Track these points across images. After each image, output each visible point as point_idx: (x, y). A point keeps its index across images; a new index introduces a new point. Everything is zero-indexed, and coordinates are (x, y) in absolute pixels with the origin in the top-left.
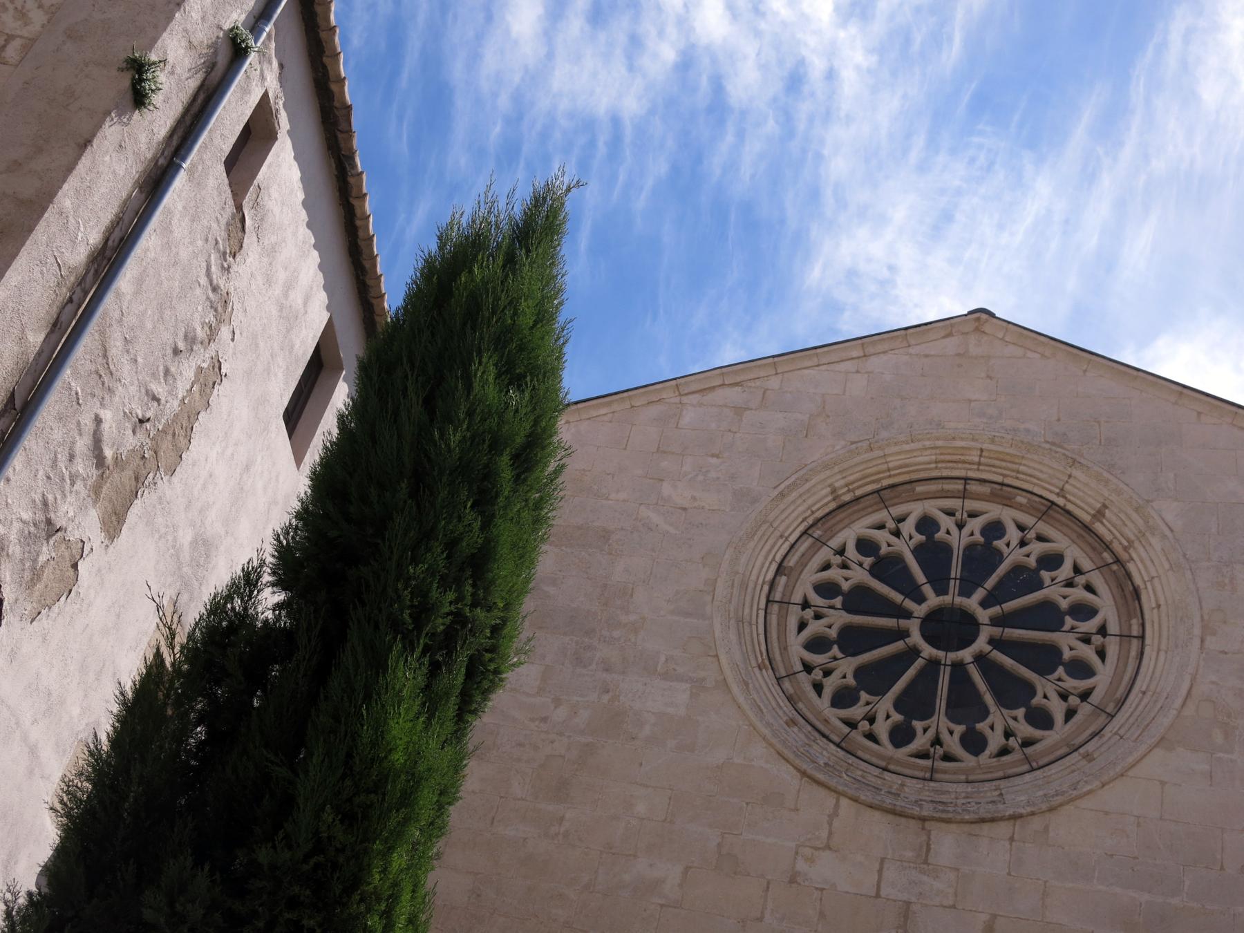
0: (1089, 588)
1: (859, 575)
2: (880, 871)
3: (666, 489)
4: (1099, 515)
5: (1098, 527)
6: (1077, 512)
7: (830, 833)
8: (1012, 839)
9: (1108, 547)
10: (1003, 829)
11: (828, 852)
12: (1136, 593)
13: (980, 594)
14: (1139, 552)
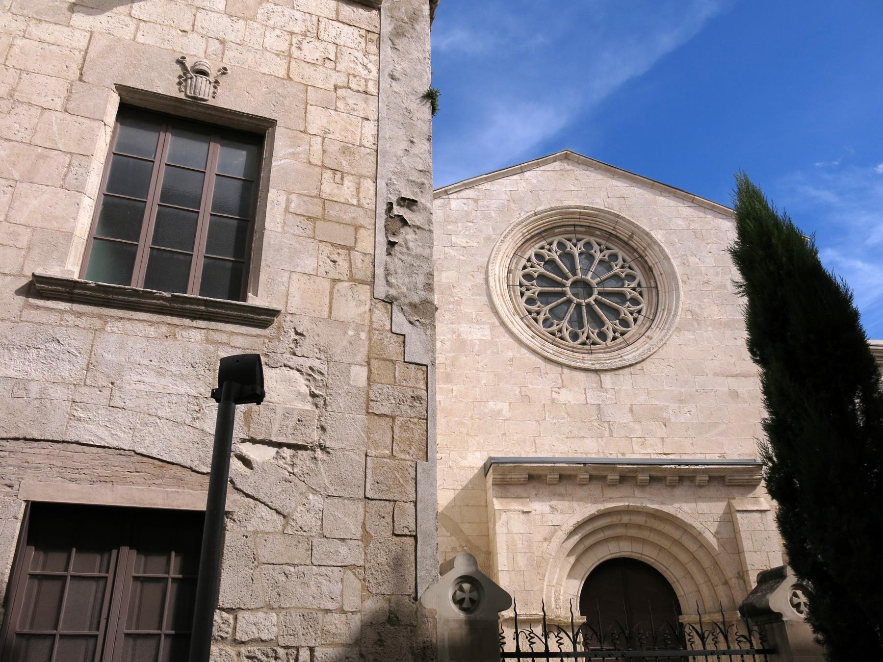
1: (541, 269)
4: (631, 237)
5: (631, 242)
6: (621, 237)
9: (636, 250)
10: (627, 370)
12: (651, 269)
13: (590, 274)
14: (649, 252)
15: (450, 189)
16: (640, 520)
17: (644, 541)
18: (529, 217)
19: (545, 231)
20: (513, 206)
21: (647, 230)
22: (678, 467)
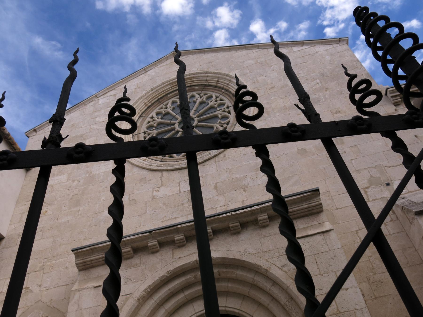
0: (221, 100)
2: (179, 186)
3: (97, 119)
5: (218, 85)
6: (212, 84)
7: (162, 182)
8: (216, 162)
9: (223, 88)
10: (212, 161)
11: (162, 187)
15: (98, 94)
18: (148, 92)
19: (161, 98)
20: (138, 90)
21: (226, 73)
22: (234, 213)
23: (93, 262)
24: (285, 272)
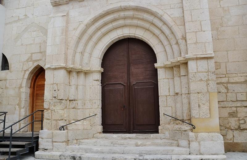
16: (130, 13)
17: (137, 26)
23: (60, 2)
24: (172, 18)
